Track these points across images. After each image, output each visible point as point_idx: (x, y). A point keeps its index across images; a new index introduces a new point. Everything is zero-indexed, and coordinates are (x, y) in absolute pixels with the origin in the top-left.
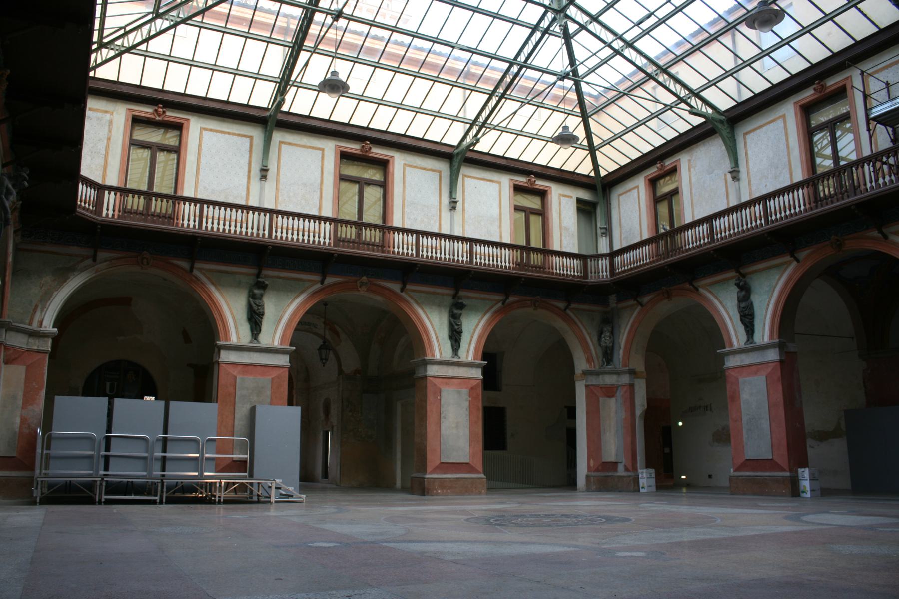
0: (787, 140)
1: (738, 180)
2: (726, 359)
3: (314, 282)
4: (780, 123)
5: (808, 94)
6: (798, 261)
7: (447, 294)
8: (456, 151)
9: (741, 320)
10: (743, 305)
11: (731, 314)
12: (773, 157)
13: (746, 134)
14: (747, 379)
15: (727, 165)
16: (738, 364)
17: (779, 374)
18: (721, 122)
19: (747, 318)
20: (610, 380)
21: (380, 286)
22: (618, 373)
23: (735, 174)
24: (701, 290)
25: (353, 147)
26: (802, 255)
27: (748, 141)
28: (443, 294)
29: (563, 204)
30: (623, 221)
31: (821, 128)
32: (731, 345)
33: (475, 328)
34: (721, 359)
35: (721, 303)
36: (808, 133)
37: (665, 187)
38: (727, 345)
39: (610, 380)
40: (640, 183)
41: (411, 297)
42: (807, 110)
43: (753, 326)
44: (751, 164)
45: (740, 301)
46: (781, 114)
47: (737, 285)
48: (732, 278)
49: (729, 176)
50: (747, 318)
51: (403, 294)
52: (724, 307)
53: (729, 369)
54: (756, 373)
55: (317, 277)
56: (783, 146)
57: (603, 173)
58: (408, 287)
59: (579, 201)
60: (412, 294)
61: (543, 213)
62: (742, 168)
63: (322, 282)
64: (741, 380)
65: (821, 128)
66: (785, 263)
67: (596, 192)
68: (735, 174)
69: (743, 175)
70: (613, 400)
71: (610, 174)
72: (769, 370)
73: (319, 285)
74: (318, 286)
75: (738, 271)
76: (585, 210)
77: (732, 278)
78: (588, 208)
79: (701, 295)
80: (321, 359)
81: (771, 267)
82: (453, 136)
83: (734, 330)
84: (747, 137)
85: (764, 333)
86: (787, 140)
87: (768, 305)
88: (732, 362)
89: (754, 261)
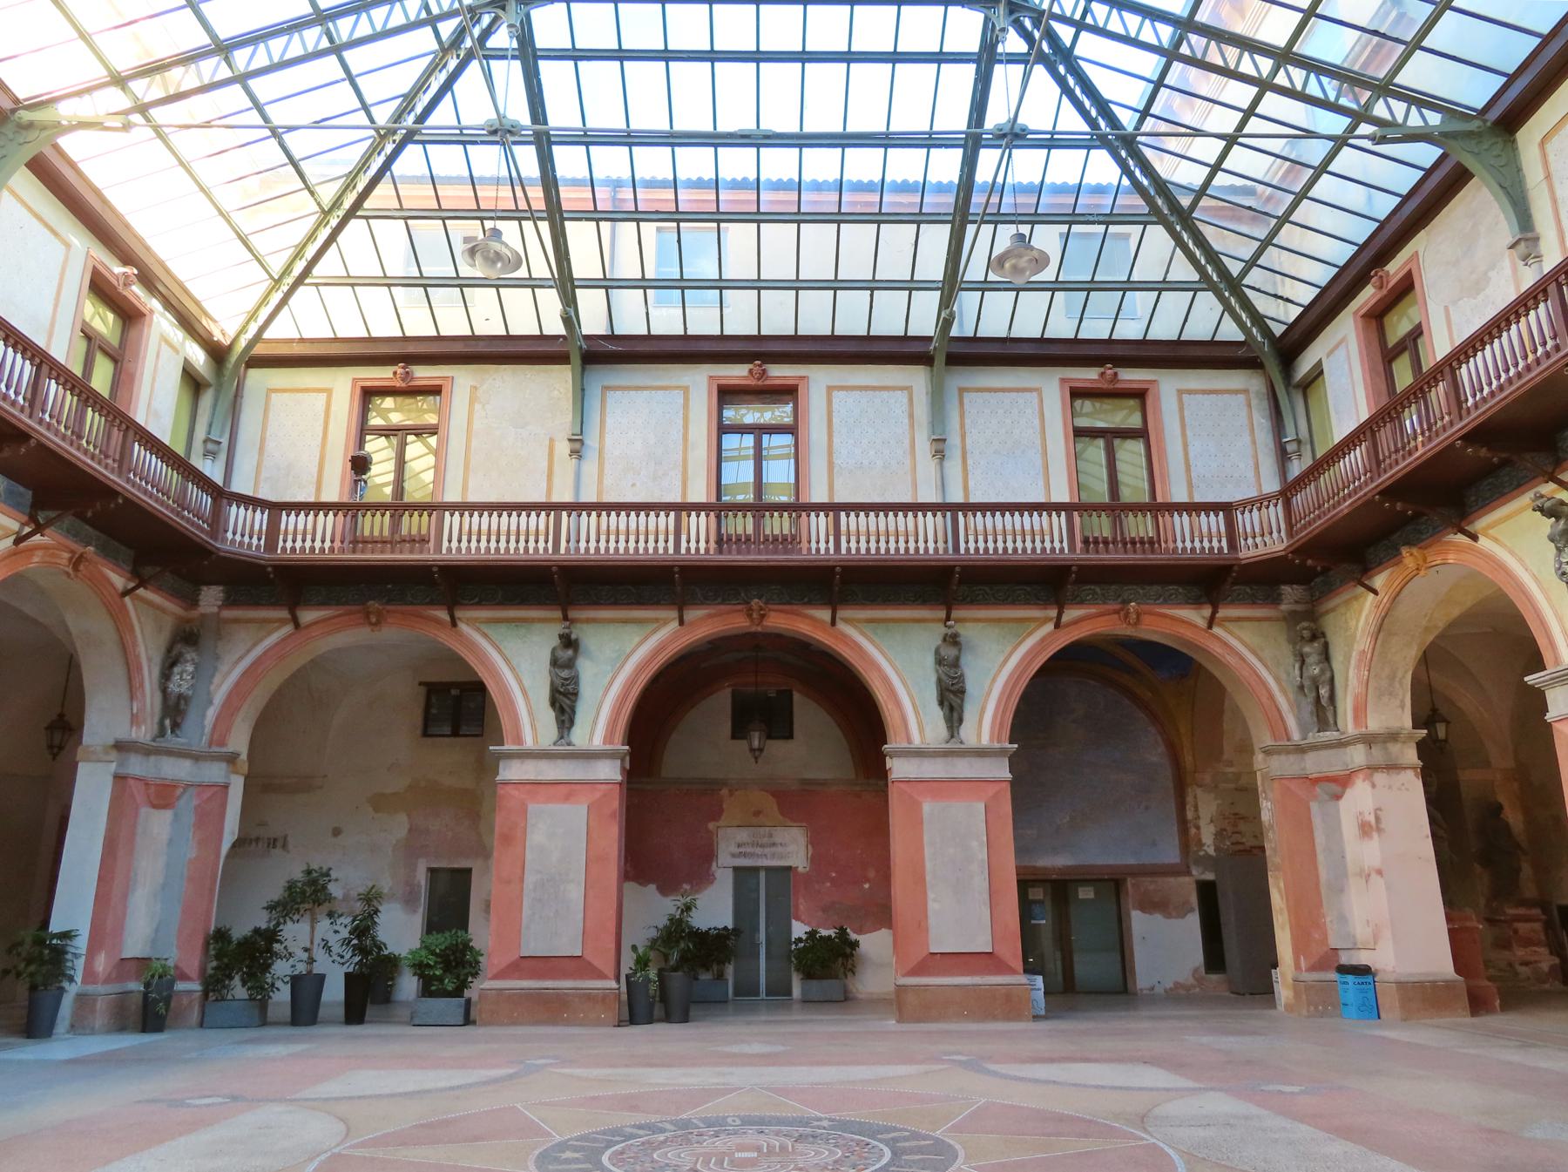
13: (606, 388)
16: (532, 777)
19: (564, 701)
20: (176, 769)
22: (197, 758)
26: (692, 614)
39: (176, 769)
43: (574, 712)
44: (608, 440)
45: (555, 662)
49: (563, 448)
50: (564, 701)
56: (676, 434)
62: (592, 440)
66: (657, 620)
70: (167, 815)
72: (598, 795)
79: (461, 635)
81: (625, 621)
84: (610, 394)
88: (511, 772)
89: (596, 603)
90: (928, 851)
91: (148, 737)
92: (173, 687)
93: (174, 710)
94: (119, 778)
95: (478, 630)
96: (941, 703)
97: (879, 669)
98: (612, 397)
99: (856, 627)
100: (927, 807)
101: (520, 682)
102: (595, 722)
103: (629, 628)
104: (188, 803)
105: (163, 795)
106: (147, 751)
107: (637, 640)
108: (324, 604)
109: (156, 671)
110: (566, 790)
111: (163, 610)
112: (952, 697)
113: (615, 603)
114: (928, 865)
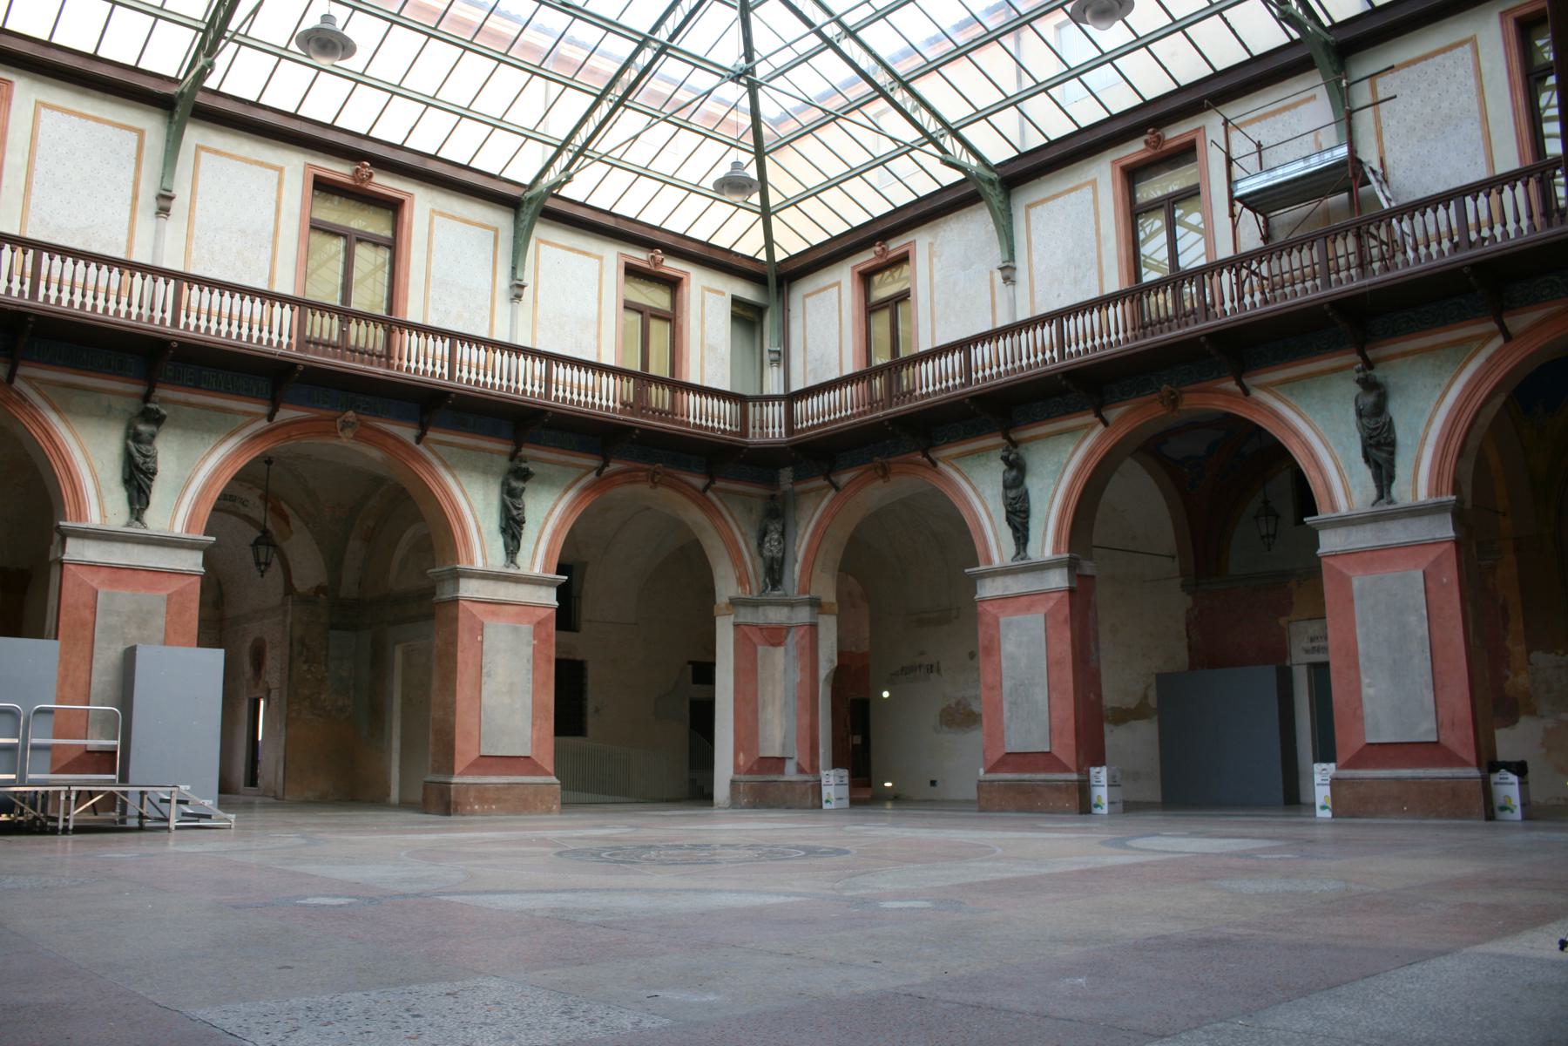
0: (1097, 222)
1: (1013, 282)
2: (979, 583)
3: (255, 417)
4: (1087, 193)
5: (1135, 150)
6: (1106, 424)
7: (499, 453)
8: (528, 195)
9: (1008, 520)
10: (1012, 494)
11: (991, 508)
12: (1072, 249)
13: (1029, 207)
14: (1015, 618)
15: (996, 256)
16: (1000, 593)
17: (1066, 610)
18: (991, 182)
19: (1018, 517)
21: (379, 431)
23: (1008, 272)
24: (941, 465)
25: (340, 170)
26: (1113, 414)
27: (1033, 218)
28: (491, 452)
29: (708, 302)
30: (809, 341)
31: (1152, 207)
32: (989, 560)
33: (548, 514)
34: (972, 583)
35: (974, 489)
36: (1134, 213)
37: (885, 288)
38: (981, 559)
40: (843, 277)
41: (433, 452)
42: (1132, 175)
44: (1035, 258)
45: (1007, 487)
46: (1090, 178)
47: (1005, 459)
48: (996, 447)
49: (998, 276)
50: (1018, 517)
51: (421, 448)
52: (979, 496)
53: (983, 600)
54: (1028, 609)
55: (261, 408)
56: (1090, 233)
57: (780, 256)
58: (431, 435)
59: (736, 301)
60: (436, 447)
61: (672, 318)
62: (1021, 263)
63: (270, 418)
64: (1002, 620)
65: (1152, 207)
66: (1086, 426)
67: (768, 287)
68: (1008, 272)
69: (1021, 275)
71: (791, 258)
72: (1051, 604)
73: (264, 423)
74: (263, 424)
75: (1006, 436)
76: (746, 317)
77: (996, 447)
78: (749, 314)
79: (940, 473)
80: (258, 564)
81: (1060, 433)
82: (523, 170)
83: (996, 535)
84: (1033, 211)
85: (1045, 541)
86: (1097, 222)
87: (1053, 496)
89: (1034, 420)
90: (1360, 632)
91: (755, 593)
92: (766, 553)
93: (774, 572)
94: (736, 626)
95: (952, 466)
96: (1367, 458)
97: (1296, 433)
98: (1035, 213)
99: (1271, 393)
100: (1357, 582)
101: (986, 508)
102: (1045, 535)
103: (1064, 439)
104: (792, 639)
105: (775, 636)
106: (755, 604)
107: (1071, 449)
108: (850, 466)
109: (754, 543)
110: (1027, 600)
111: (750, 495)
112: (1380, 451)
113: (1049, 417)
114: (1361, 646)
